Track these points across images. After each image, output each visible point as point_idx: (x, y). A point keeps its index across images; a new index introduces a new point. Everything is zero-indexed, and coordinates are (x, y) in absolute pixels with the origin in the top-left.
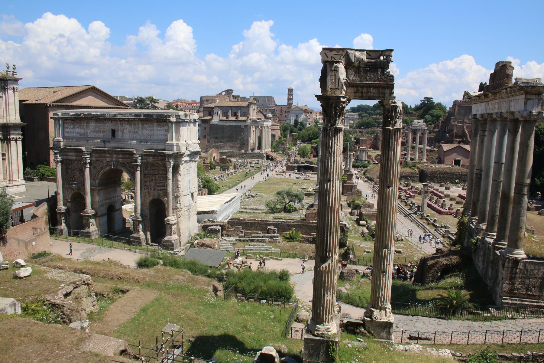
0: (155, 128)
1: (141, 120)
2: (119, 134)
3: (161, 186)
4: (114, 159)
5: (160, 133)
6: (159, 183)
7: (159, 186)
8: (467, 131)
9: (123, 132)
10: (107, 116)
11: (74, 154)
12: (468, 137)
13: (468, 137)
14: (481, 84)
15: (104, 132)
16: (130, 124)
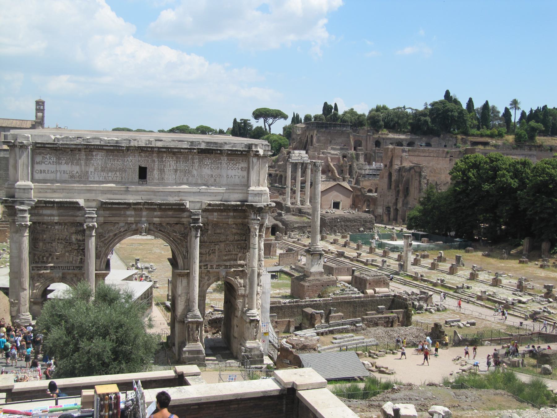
0: (224, 165)
1: (202, 152)
2: (154, 174)
3: (229, 260)
4: (144, 219)
5: (231, 173)
6: (226, 255)
7: (225, 261)
8: (331, 164)
9: (162, 171)
10: (132, 144)
11: (55, 212)
12: (336, 171)
13: (336, 171)
14: (326, 104)
15: (123, 170)
16: (177, 158)
